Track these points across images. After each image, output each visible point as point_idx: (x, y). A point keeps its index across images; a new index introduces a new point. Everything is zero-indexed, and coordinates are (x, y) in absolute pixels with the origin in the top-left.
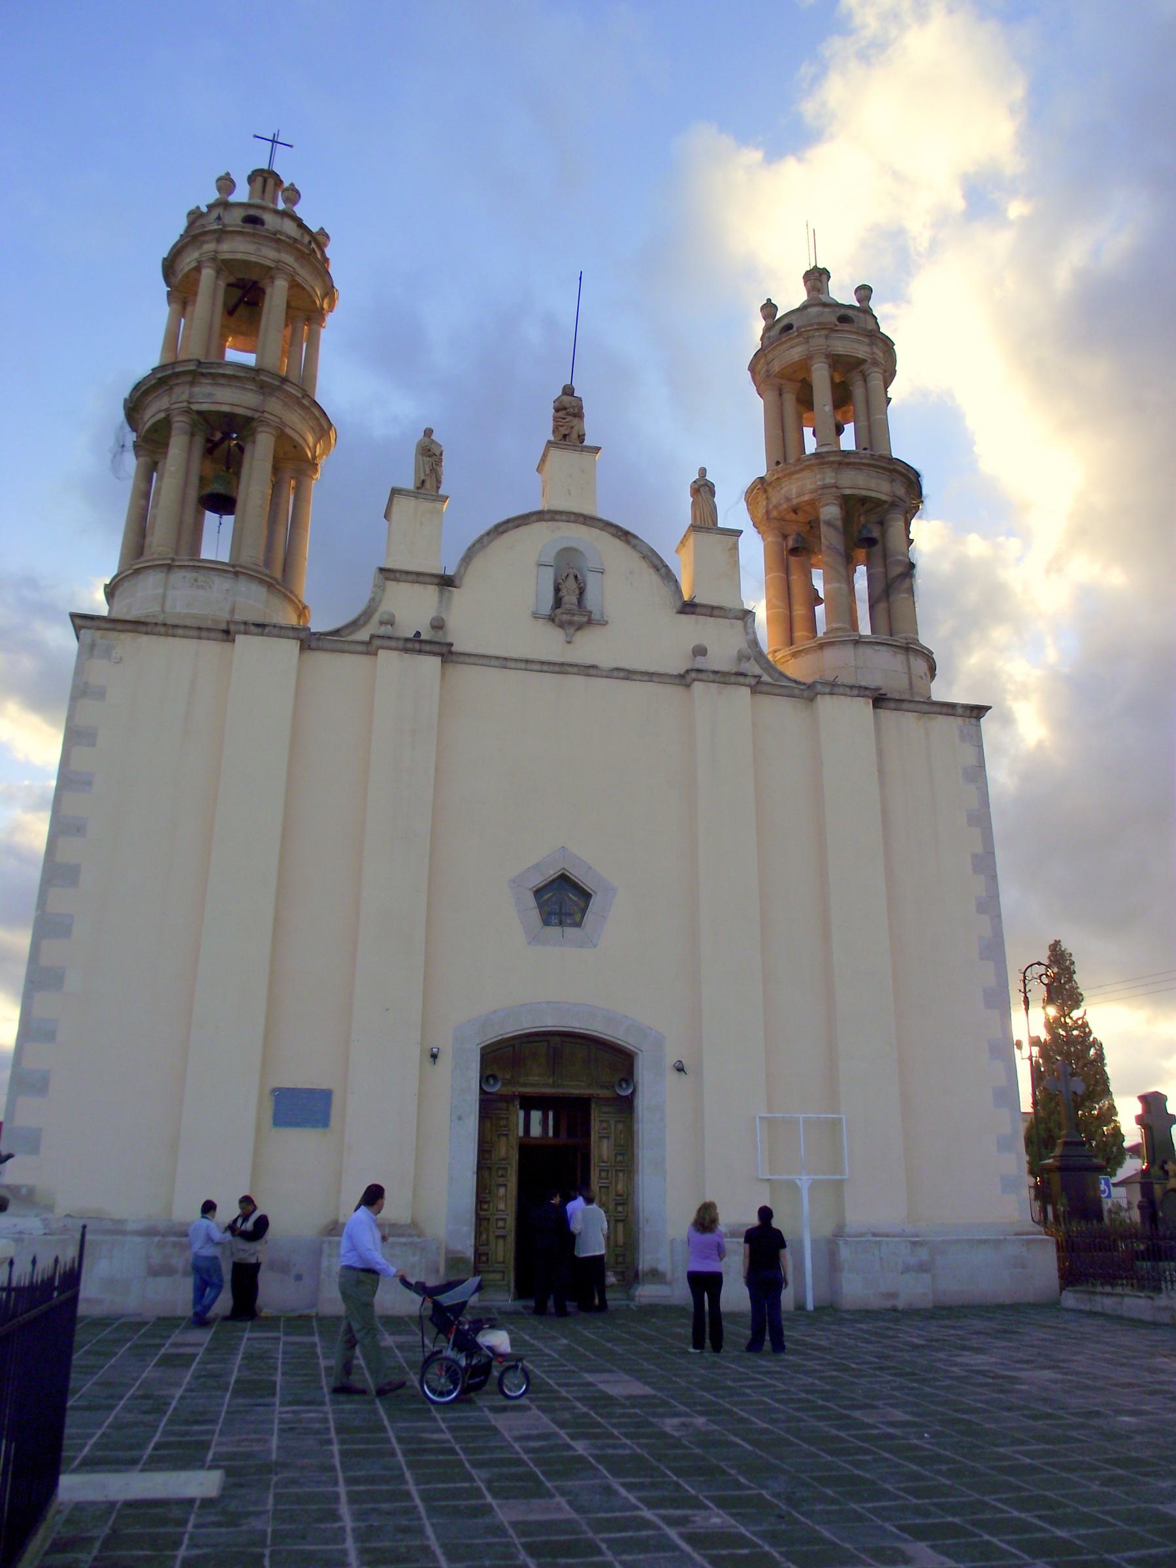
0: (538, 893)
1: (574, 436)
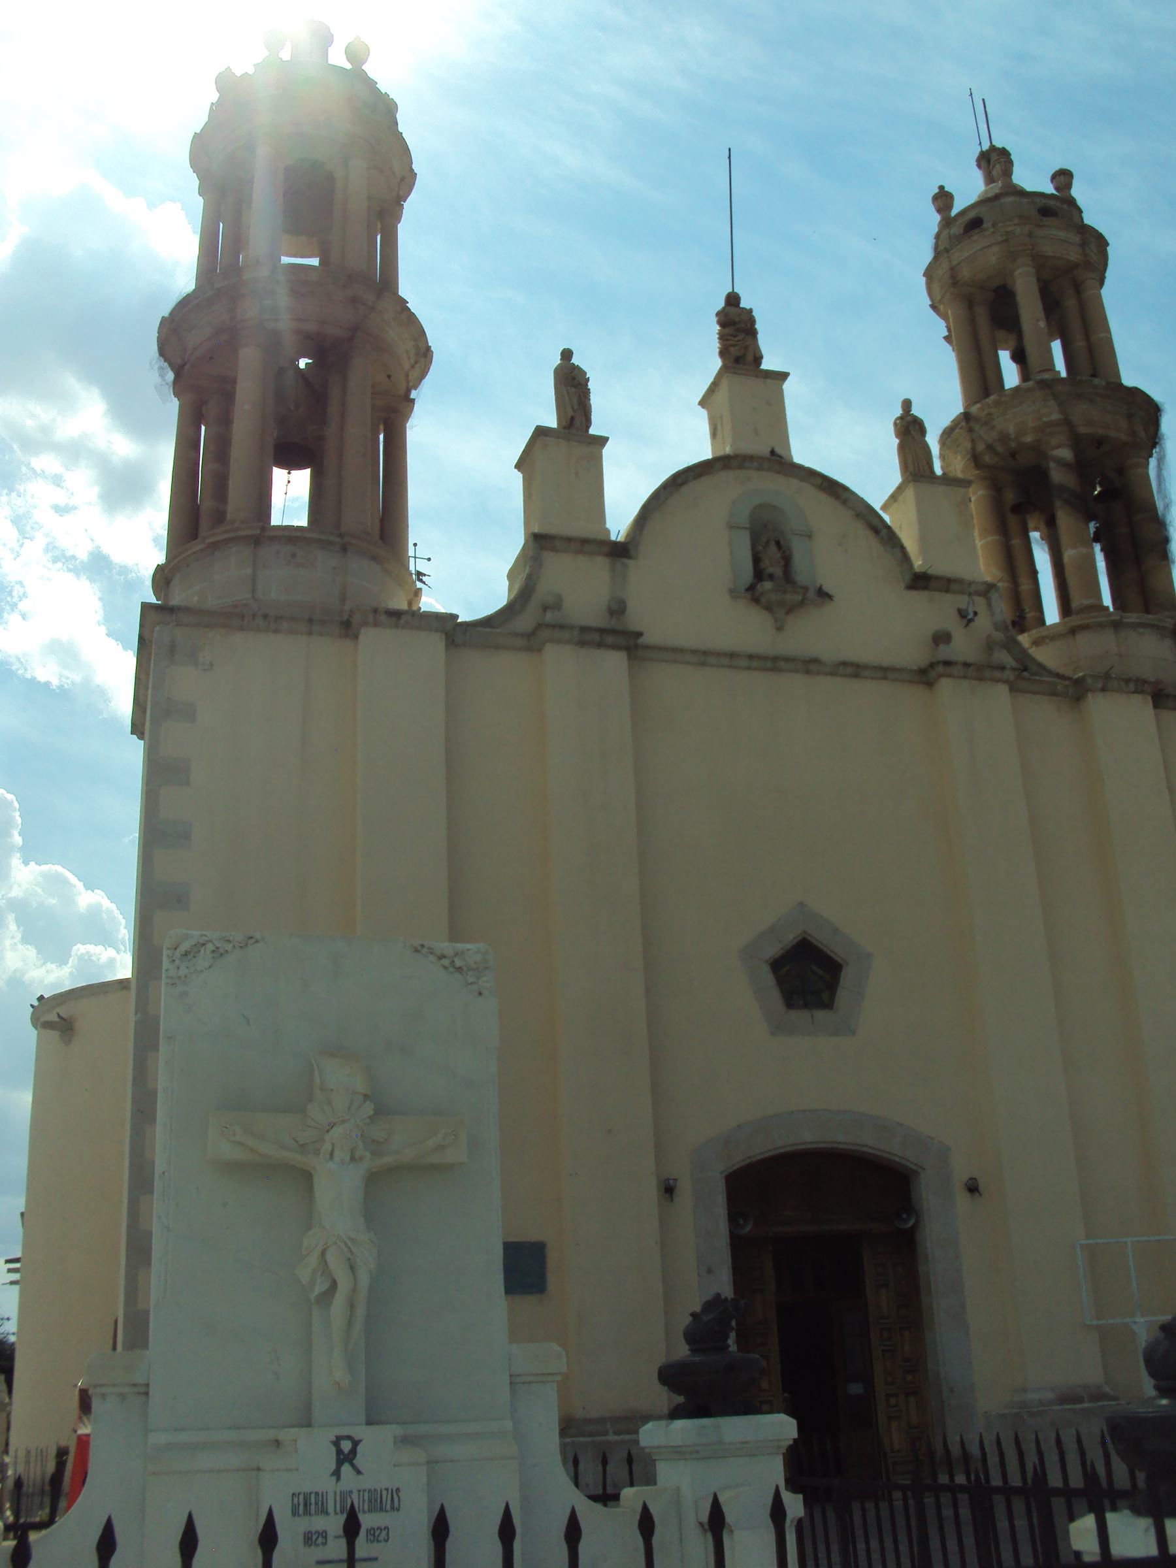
0: (776, 965)
1: (750, 358)
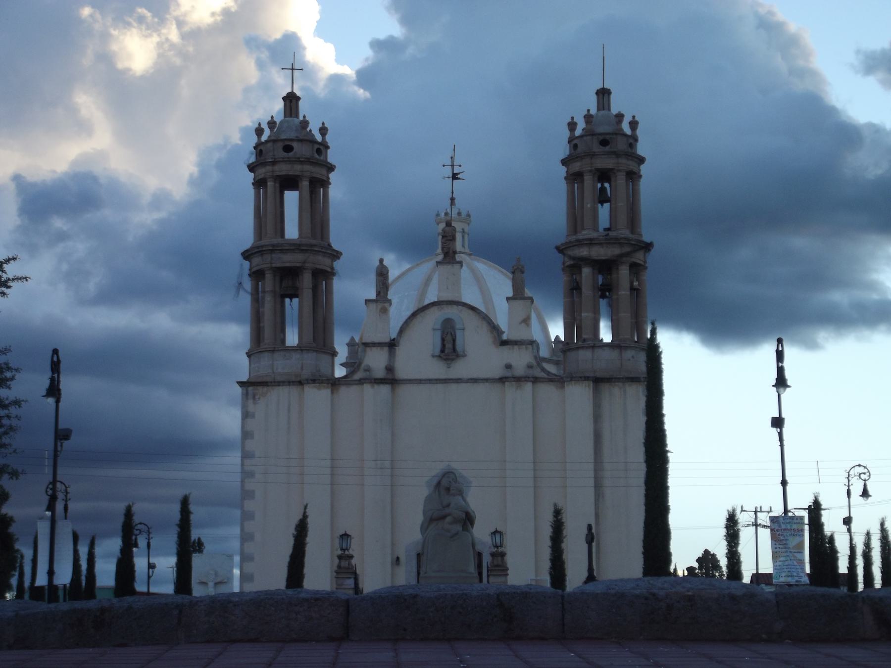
1: (451, 252)
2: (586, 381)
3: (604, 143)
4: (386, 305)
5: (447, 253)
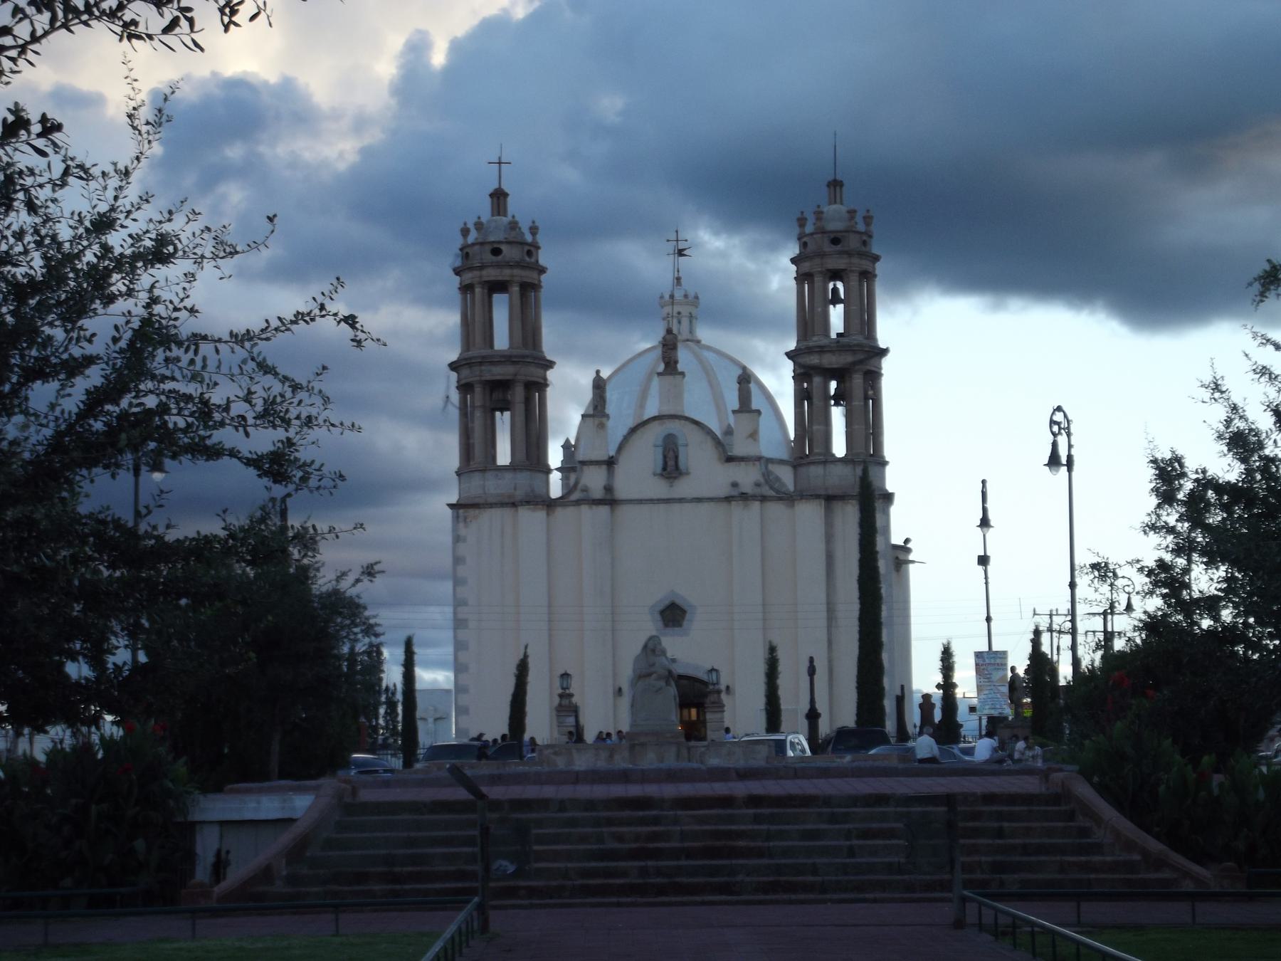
1: (672, 362)
2: (818, 500)
3: (835, 241)
4: (604, 420)
5: (668, 363)
